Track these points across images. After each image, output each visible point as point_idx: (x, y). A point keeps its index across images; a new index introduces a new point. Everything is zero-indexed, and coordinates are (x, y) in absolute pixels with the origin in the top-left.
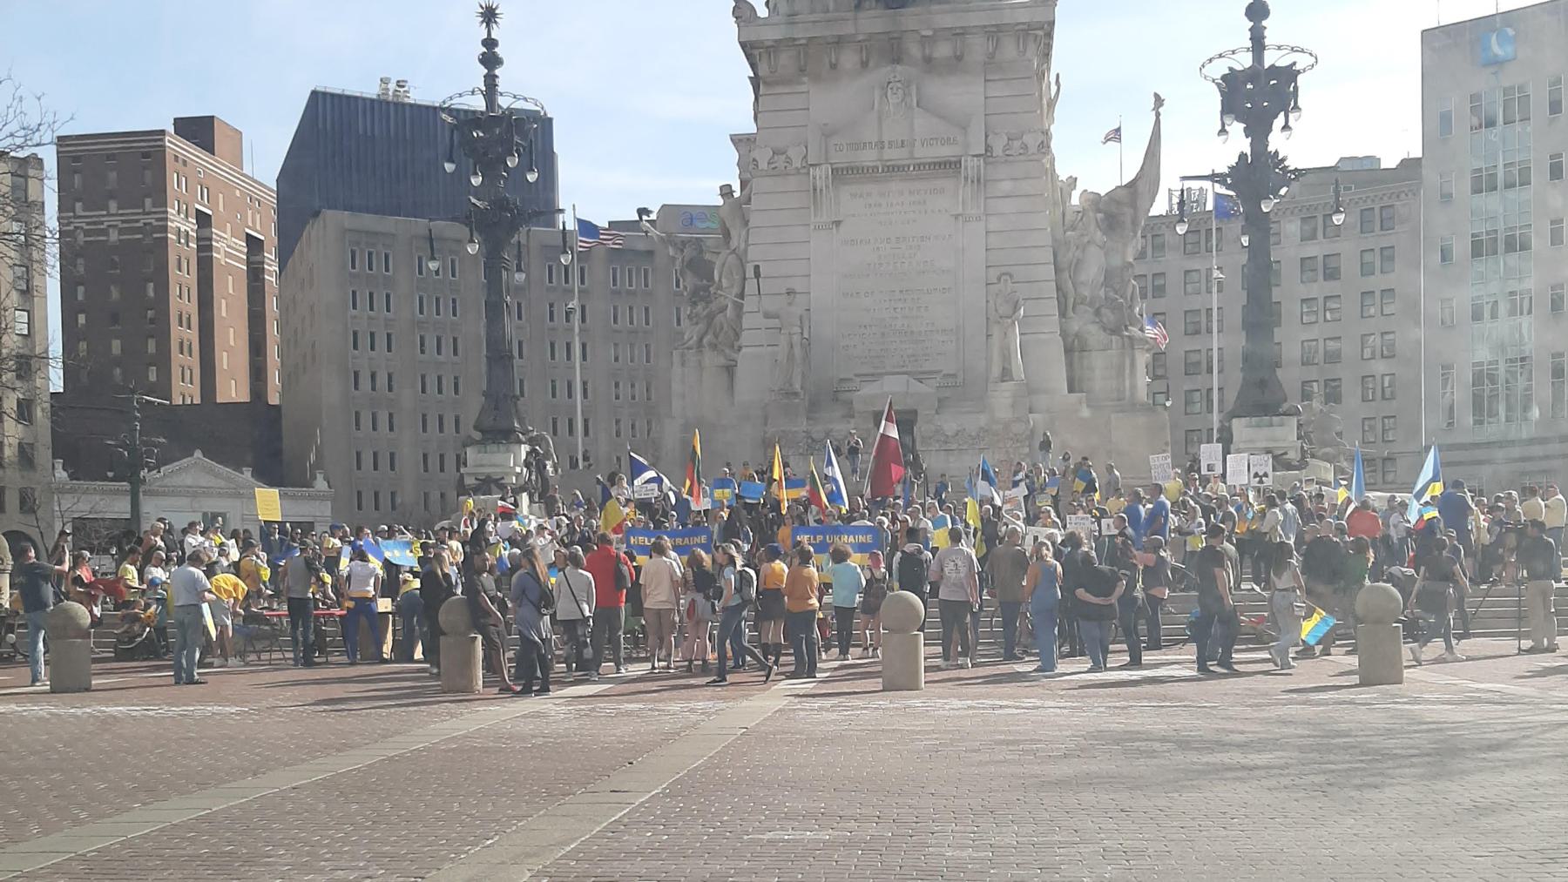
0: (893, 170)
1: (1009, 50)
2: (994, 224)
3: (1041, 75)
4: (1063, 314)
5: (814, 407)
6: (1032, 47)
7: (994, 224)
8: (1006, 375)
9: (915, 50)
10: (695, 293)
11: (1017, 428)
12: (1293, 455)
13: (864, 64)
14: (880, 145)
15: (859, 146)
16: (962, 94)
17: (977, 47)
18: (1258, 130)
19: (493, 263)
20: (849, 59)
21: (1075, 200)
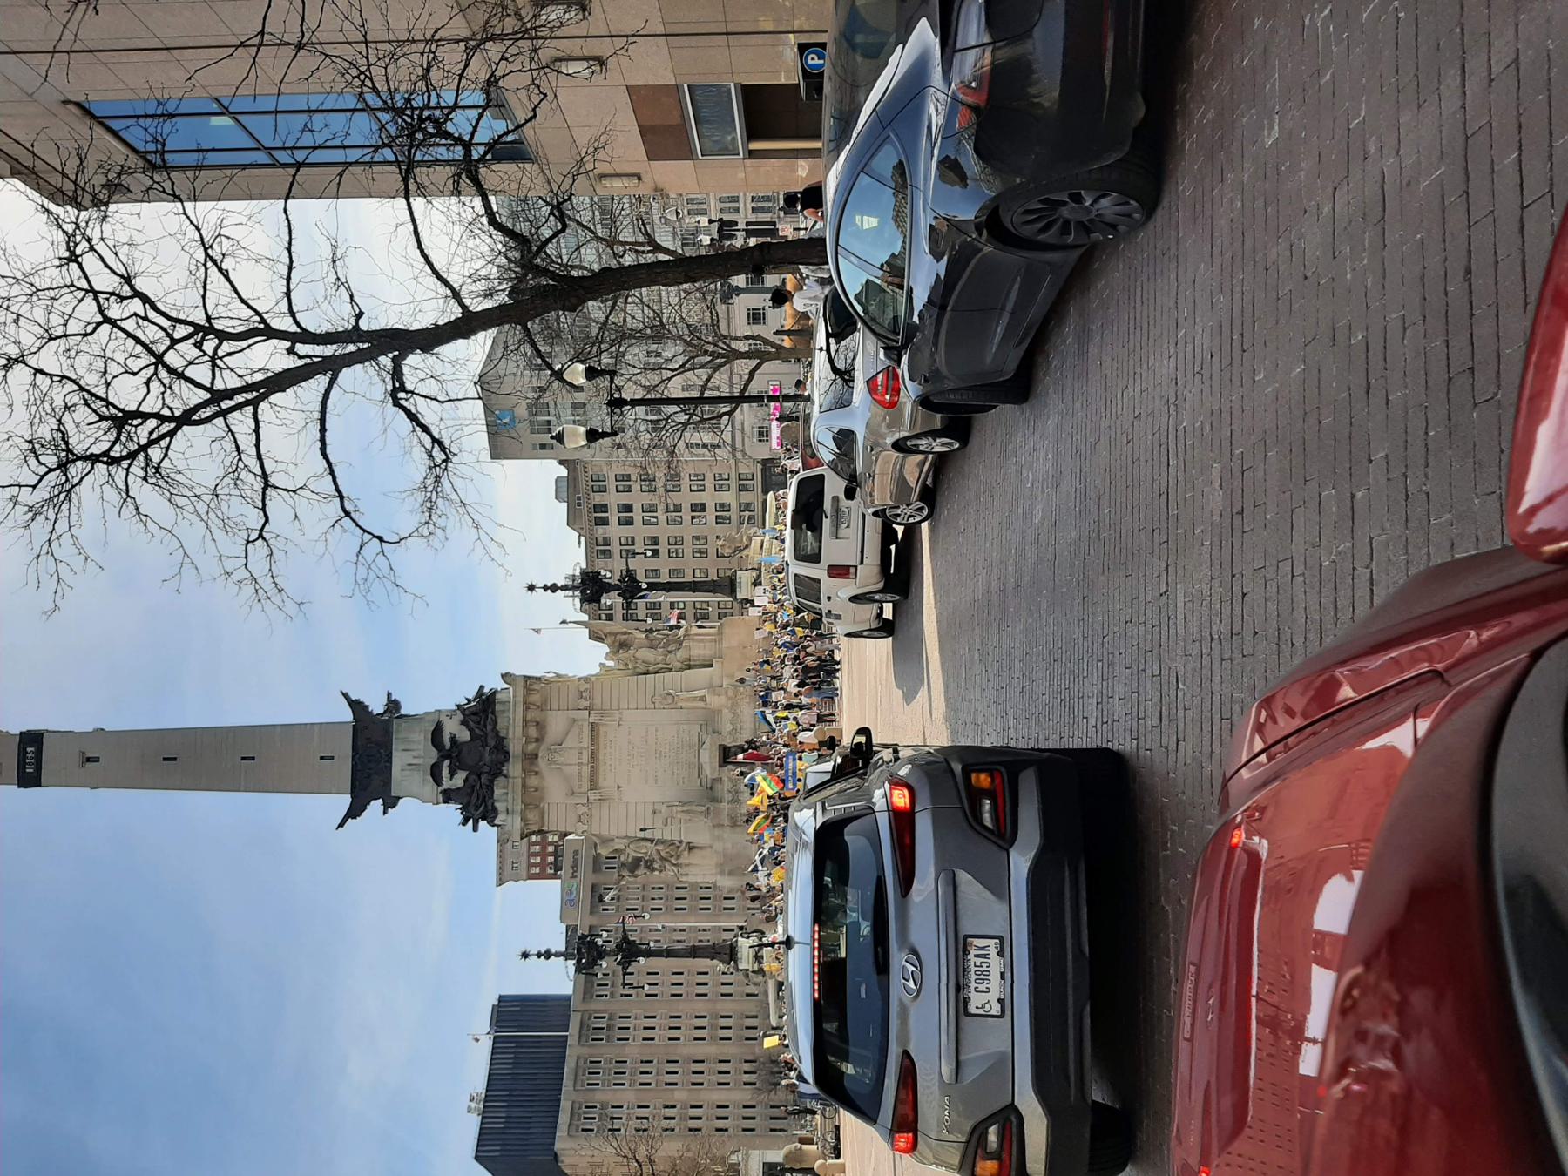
0: (593, 757)
1: (535, 698)
3: (548, 682)
4: (670, 670)
5: (714, 800)
6: (536, 687)
8: (703, 699)
9: (531, 747)
10: (648, 867)
11: (730, 694)
12: (755, 573)
13: (537, 773)
14: (580, 764)
15: (580, 778)
16: (556, 723)
17: (533, 714)
18: (608, 588)
19: (649, 953)
20: (533, 781)
21: (611, 663)
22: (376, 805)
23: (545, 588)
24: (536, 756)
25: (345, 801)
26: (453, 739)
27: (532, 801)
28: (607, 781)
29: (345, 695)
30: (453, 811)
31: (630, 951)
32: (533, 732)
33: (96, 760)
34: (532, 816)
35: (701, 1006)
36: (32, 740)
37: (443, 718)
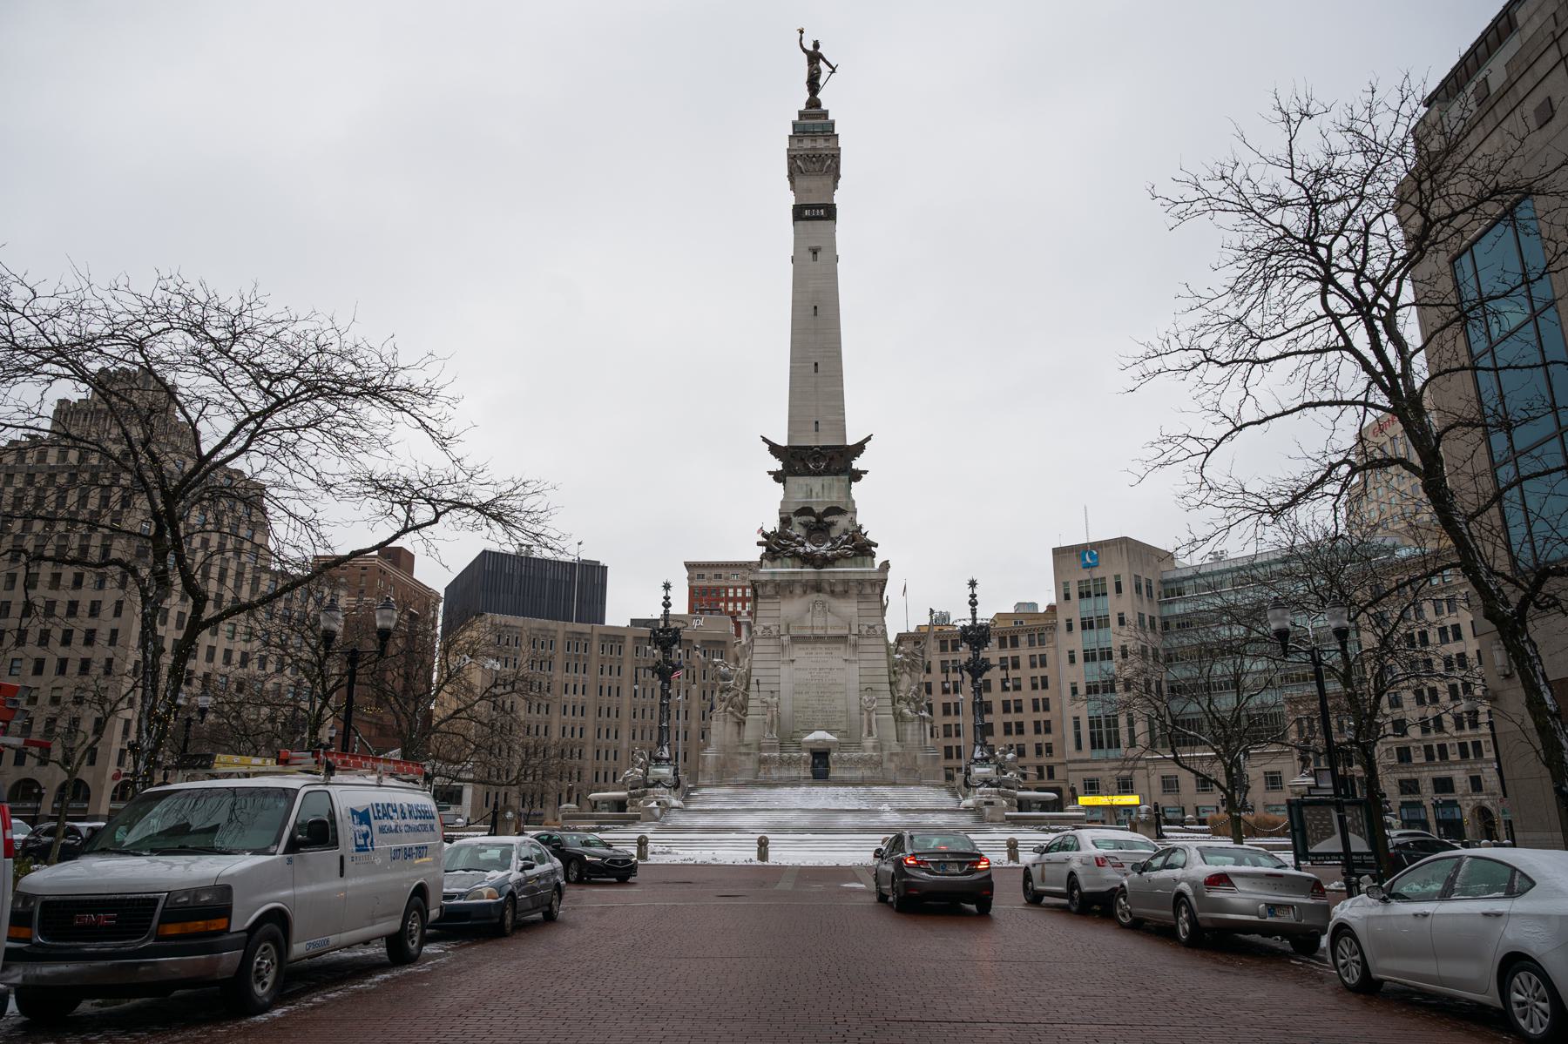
0: (818, 639)
2: (863, 664)
7: (863, 664)
8: (870, 733)
15: (802, 628)
20: (798, 590)
22: (777, 465)
23: (973, 596)
24: (819, 591)
25: (783, 442)
26: (832, 524)
27: (783, 589)
28: (798, 652)
29: (869, 438)
30: (772, 524)
31: (664, 672)
32: (839, 588)
33: (815, 259)
34: (769, 590)
35: (590, 733)
36: (830, 212)
37: (849, 516)
